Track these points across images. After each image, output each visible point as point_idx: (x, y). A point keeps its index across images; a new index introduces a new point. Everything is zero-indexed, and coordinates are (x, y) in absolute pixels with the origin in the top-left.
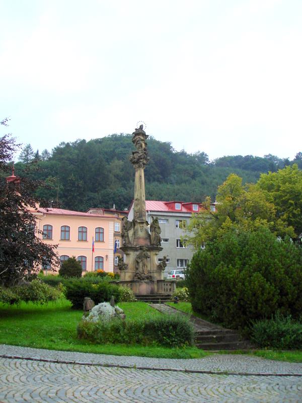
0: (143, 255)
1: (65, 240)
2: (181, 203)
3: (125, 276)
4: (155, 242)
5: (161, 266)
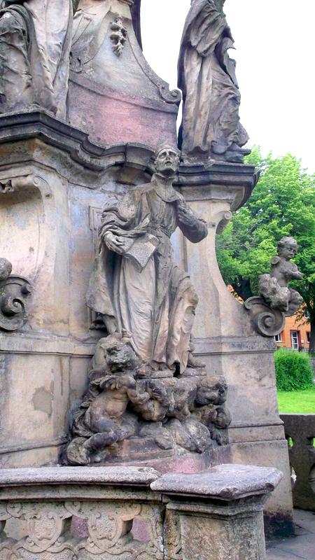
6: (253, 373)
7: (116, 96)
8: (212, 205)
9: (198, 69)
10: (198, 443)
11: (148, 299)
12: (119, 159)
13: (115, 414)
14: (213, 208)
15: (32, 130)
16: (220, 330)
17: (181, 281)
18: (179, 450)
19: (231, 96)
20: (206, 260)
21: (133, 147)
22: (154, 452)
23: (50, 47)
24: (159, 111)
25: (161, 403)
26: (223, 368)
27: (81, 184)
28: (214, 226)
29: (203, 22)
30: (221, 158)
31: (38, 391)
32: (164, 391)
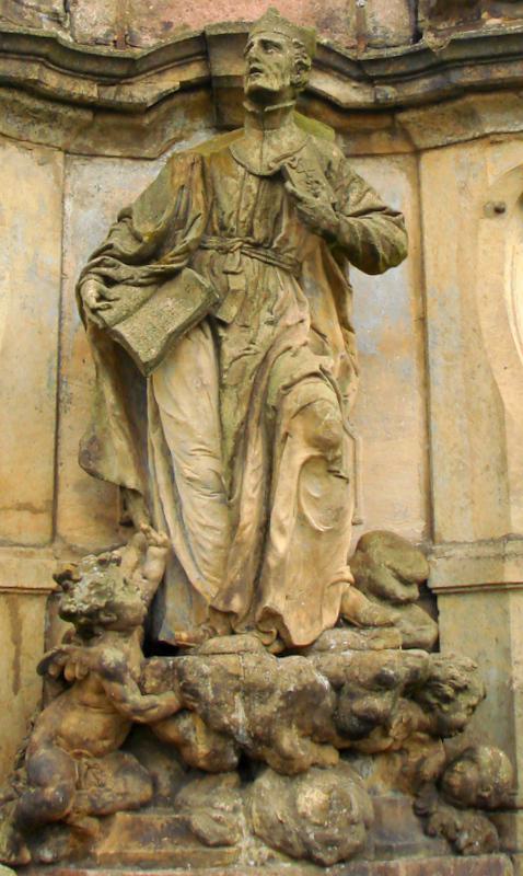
0: (238, 195)
10: (312, 837)
11: (202, 443)
12: (193, 73)
13: (84, 744)
14: (495, 162)
17: (285, 388)
18: (255, 852)
20: (475, 313)
22: (178, 850)
25: (205, 719)
27: (107, 152)
28: (499, 211)
32: (207, 690)
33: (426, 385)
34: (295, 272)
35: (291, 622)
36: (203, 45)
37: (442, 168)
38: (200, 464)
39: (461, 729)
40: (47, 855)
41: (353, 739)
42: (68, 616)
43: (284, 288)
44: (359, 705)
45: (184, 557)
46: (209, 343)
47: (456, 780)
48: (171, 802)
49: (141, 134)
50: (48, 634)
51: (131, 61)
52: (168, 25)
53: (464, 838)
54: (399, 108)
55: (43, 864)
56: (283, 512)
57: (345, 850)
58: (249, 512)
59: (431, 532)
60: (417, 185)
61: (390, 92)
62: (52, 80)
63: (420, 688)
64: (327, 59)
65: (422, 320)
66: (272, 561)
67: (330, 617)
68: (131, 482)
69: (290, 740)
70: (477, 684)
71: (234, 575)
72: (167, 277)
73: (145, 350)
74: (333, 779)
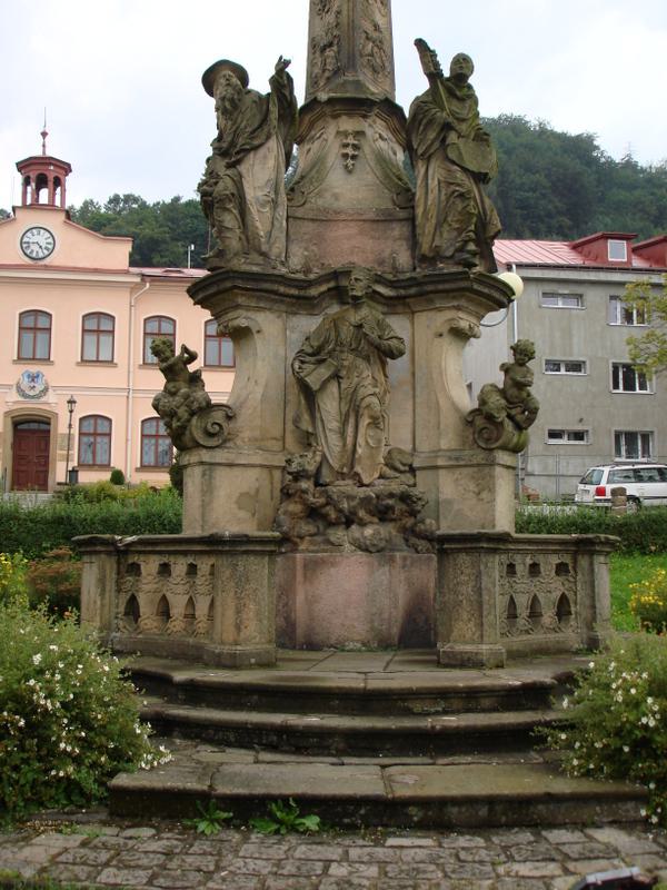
0: (347, 332)
1: (219, 366)
2: (627, 238)
3: (208, 490)
4: (447, 241)
5: (490, 418)
6: (472, 487)
7: (343, 217)
8: (439, 314)
9: (423, 171)
12: (332, 284)
13: (296, 514)
15: (228, 284)
16: (439, 443)
19: (456, 194)
21: (341, 273)
23: (258, 199)
24: (391, 221)
26: (441, 480)
28: (441, 335)
29: (420, 124)
30: (450, 262)
31: (242, 495)
32: (335, 497)
33: (414, 397)
34: (367, 359)
35: (363, 477)
36: (335, 275)
37: (422, 319)
38: (333, 424)
39: (419, 512)
40: (283, 550)
41: (383, 514)
42: (289, 473)
43: (362, 364)
44: (384, 503)
45: (327, 454)
46: (336, 384)
47: (417, 529)
48: (324, 534)
49: (313, 307)
50: (282, 482)
51: (310, 281)
52: (323, 264)
53: (420, 548)
54: (405, 297)
55: (282, 553)
56: (361, 440)
57: (379, 548)
58: (349, 440)
59: (414, 449)
60: (413, 324)
61: (402, 292)
62: (282, 289)
63: (404, 498)
64: (379, 280)
65: (413, 374)
66: (357, 456)
67: (377, 475)
68: (310, 430)
69: (362, 513)
70: (425, 498)
71: (344, 461)
72: (324, 361)
73: (315, 387)
74: (376, 527)
